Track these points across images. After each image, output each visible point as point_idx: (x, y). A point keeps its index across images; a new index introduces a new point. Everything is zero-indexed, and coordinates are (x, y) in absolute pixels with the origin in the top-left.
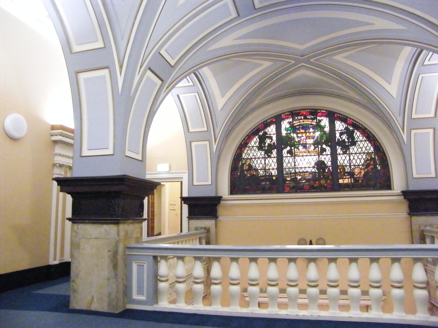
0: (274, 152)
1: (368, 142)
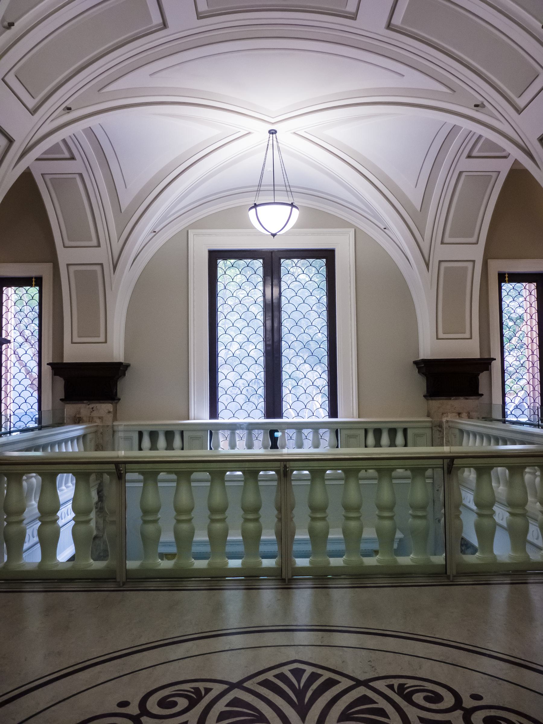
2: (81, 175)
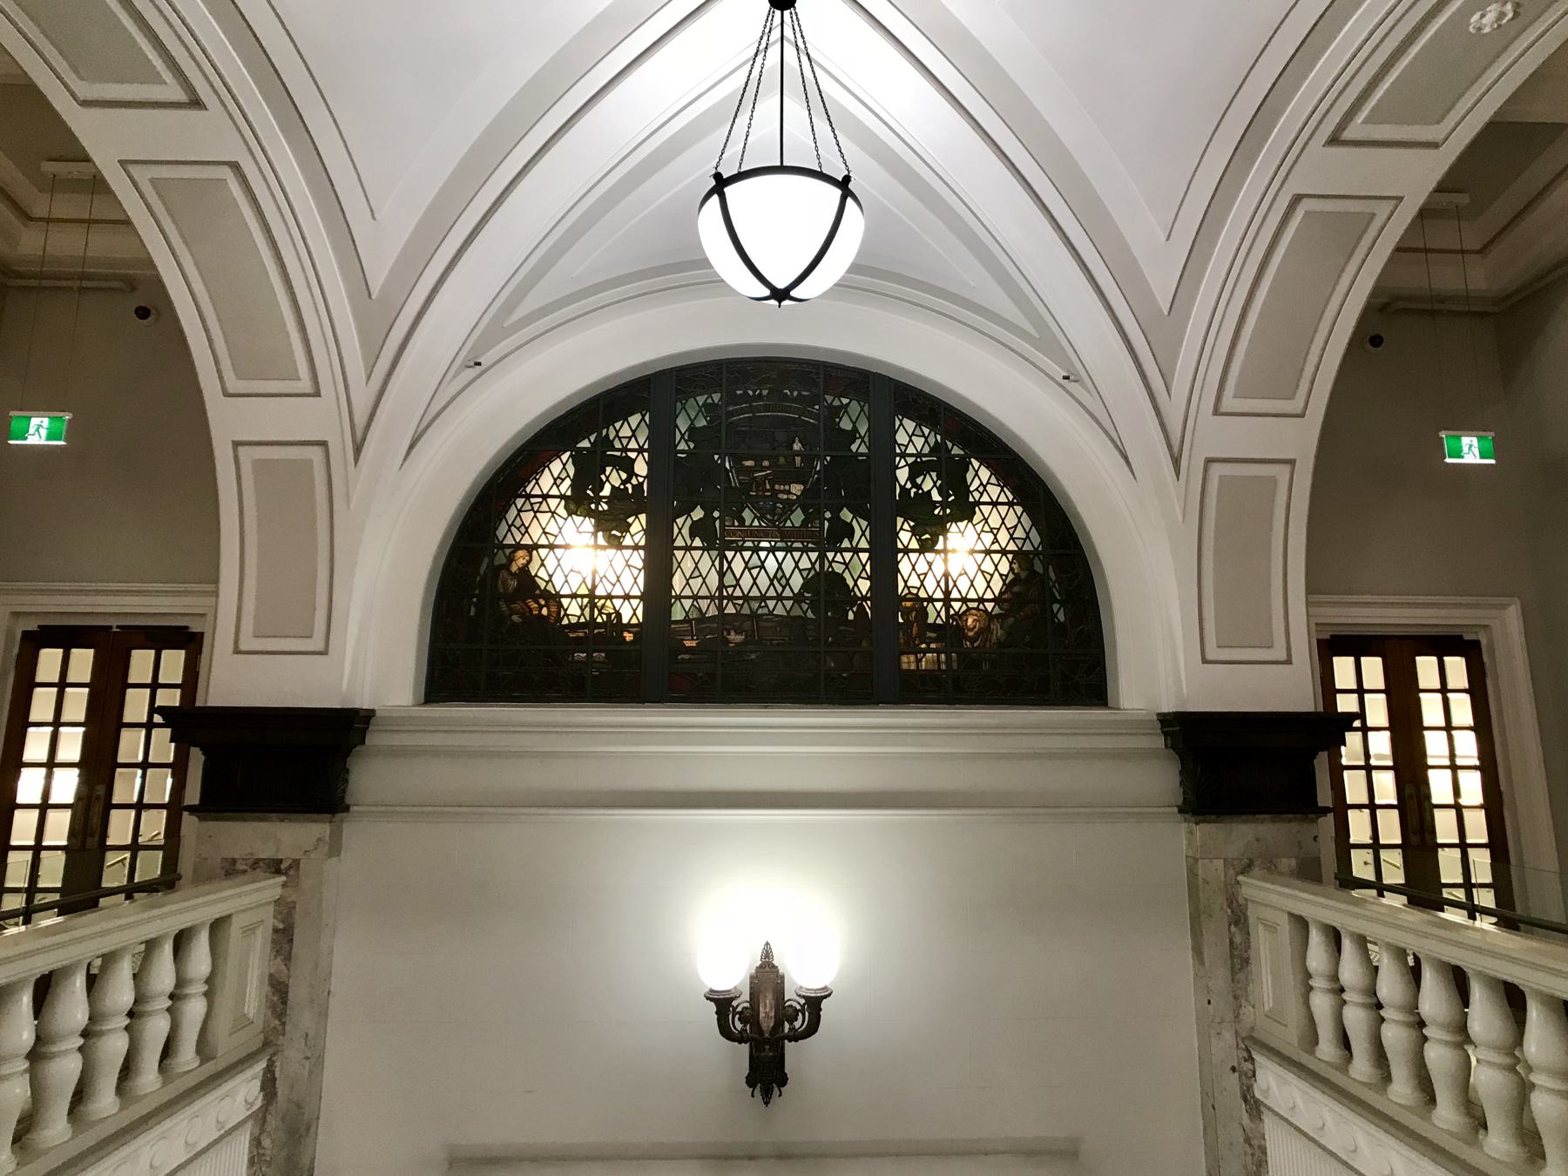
0: (638, 525)
1: (1019, 509)
2: (235, 166)
